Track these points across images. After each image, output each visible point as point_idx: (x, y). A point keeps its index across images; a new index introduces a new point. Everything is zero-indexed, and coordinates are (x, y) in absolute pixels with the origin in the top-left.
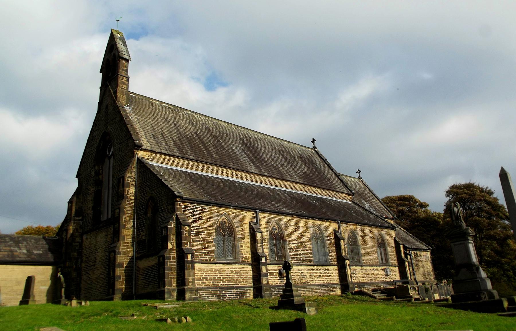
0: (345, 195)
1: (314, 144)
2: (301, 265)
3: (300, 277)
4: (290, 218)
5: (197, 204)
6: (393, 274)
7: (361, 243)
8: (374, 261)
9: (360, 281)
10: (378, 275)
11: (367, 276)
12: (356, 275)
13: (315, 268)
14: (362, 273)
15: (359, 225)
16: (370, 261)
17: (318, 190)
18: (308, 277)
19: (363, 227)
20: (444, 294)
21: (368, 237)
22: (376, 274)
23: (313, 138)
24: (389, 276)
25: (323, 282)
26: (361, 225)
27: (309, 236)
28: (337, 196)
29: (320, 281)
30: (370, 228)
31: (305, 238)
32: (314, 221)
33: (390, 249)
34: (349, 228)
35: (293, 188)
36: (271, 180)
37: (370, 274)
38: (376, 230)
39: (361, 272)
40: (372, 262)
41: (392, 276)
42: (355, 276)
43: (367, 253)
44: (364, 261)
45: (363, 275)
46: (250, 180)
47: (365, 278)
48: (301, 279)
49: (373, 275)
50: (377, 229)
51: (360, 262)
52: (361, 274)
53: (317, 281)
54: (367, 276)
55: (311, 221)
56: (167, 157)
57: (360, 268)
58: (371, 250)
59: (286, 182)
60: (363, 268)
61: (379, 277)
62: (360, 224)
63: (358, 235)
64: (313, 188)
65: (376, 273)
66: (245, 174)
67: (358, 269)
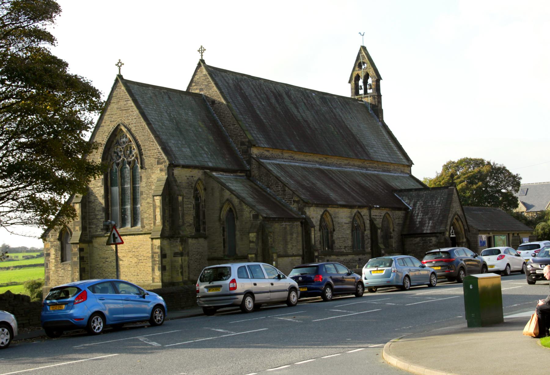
1: (202, 55)
23: (202, 46)
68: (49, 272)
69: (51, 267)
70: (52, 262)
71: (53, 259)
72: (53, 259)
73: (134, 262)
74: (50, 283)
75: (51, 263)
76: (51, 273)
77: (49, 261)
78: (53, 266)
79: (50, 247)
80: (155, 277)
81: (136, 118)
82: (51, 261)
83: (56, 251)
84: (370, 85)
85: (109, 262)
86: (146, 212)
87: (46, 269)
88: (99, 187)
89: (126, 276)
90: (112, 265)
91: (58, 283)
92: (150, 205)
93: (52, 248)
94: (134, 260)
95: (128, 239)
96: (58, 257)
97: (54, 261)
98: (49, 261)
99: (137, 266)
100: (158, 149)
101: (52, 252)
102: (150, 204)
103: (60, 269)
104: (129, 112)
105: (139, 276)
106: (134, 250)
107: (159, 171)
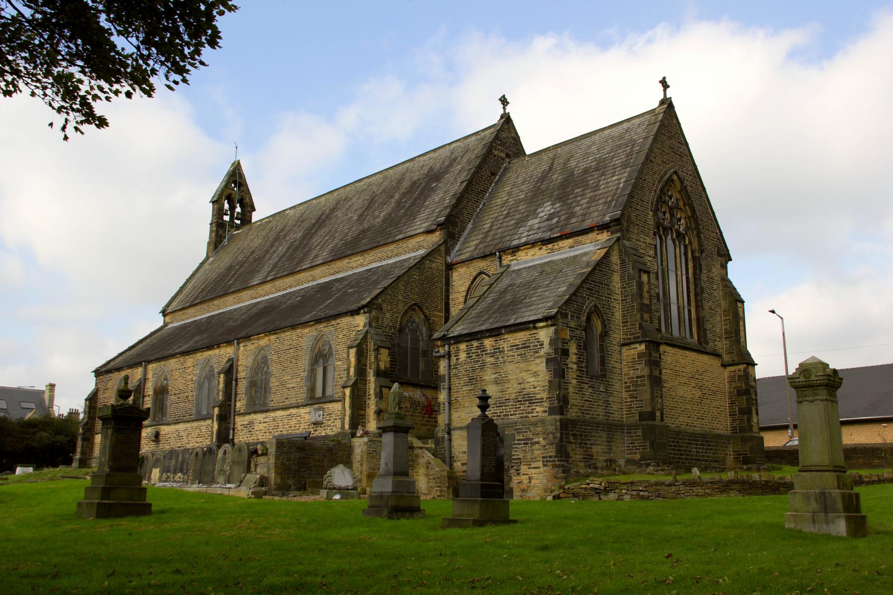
0: (421, 238)
2: (179, 423)
3: (176, 440)
4: (176, 360)
5: (106, 374)
6: (336, 419)
7: (274, 368)
8: (295, 397)
9: (258, 439)
10: (298, 424)
11: (273, 429)
12: (253, 429)
13: (195, 424)
14: (265, 425)
15: (272, 332)
16: (286, 399)
17: (356, 259)
18: (185, 438)
19: (283, 335)
20: (172, 468)
21: (291, 351)
22: (293, 423)
24: (323, 425)
25: (201, 444)
26: (275, 332)
27: (194, 379)
28: (400, 250)
29: (198, 443)
30: (299, 331)
31: (189, 383)
32: (204, 353)
33: (340, 363)
34: (256, 345)
35: (311, 278)
36: (278, 283)
37: (280, 425)
38: (310, 330)
39: (264, 423)
40: (289, 401)
41: (334, 422)
42: (251, 431)
43: (283, 384)
44: (273, 401)
45: (265, 427)
46: (252, 298)
47: (269, 432)
48: (177, 442)
49: (286, 426)
50: (313, 328)
51: (265, 404)
52: (261, 426)
53: (195, 444)
54: (273, 429)
55: (200, 354)
56: (182, 312)
57: (264, 415)
58: (292, 376)
59: (299, 275)
60: (268, 414)
61: (298, 429)
62: (256, 335)
63: (271, 353)
64: (346, 261)
65: (293, 422)
66: (247, 292)
67: (260, 417)
68: (567, 389)
69: (571, 377)
70: (572, 369)
71: (575, 363)
72: (575, 363)
73: (697, 396)
74: (568, 411)
75: (570, 370)
76: (571, 390)
77: (567, 365)
78: (575, 376)
79: (568, 337)
80: (753, 423)
81: (691, 175)
82: (569, 366)
83: (579, 349)
84: (238, 213)
85: (667, 389)
86: (709, 321)
87: (562, 380)
88: (650, 256)
89: (688, 417)
90: (671, 395)
91: (583, 413)
92: (712, 311)
93: (572, 342)
94: (698, 394)
95: (690, 357)
96: (583, 362)
97: (575, 366)
98: (567, 365)
99: (701, 403)
100: (717, 233)
101: (573, 349)
102: (713, 310)
103: (586, 386)
104: (683, 161)
105: (703, 419)
106: (697, 376)
107: (719, 266)
